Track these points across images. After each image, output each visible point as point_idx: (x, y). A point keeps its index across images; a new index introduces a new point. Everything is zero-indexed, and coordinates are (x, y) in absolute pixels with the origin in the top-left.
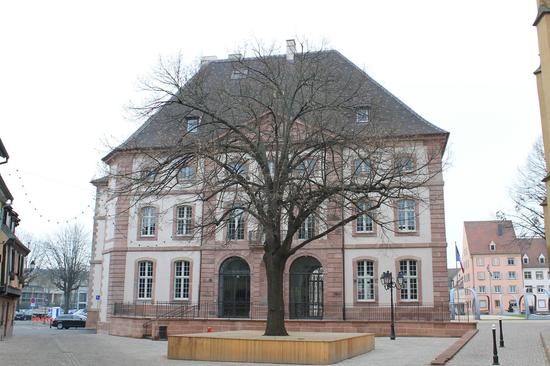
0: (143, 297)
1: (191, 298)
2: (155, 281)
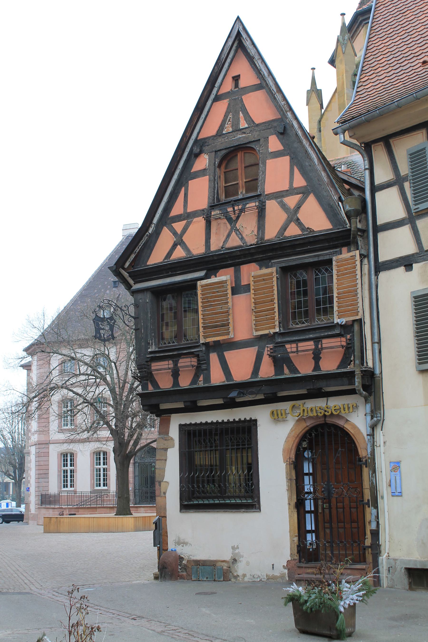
0: (67, 487)
1: (110, 487)
2: (76, 472)
